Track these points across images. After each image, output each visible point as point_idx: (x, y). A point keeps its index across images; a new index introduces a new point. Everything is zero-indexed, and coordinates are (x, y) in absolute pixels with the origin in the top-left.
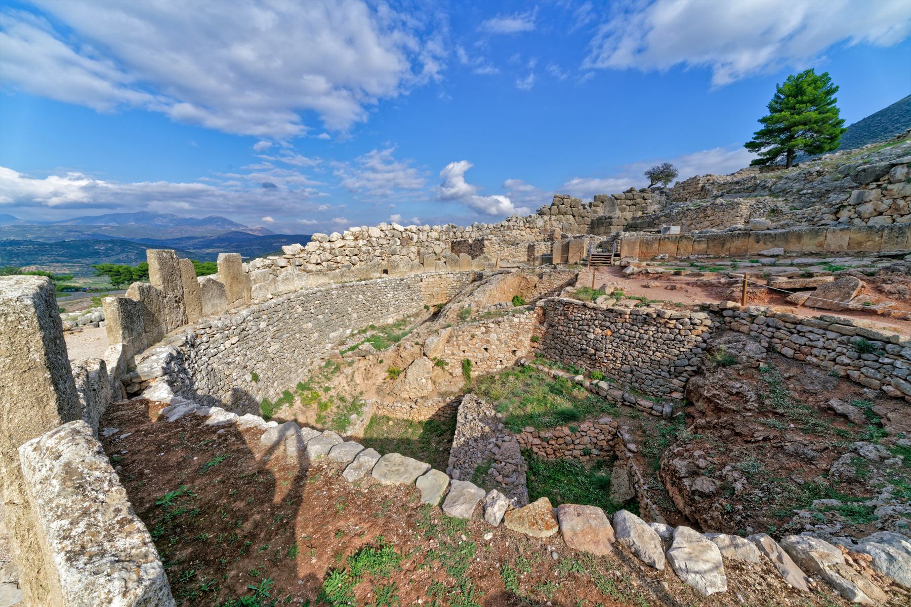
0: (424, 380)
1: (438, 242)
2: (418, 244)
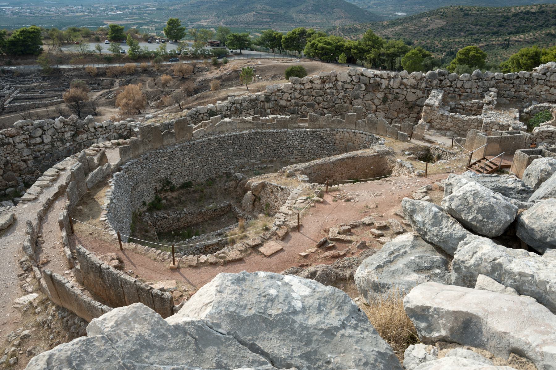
1: (413, 90)
2: (386, 91)
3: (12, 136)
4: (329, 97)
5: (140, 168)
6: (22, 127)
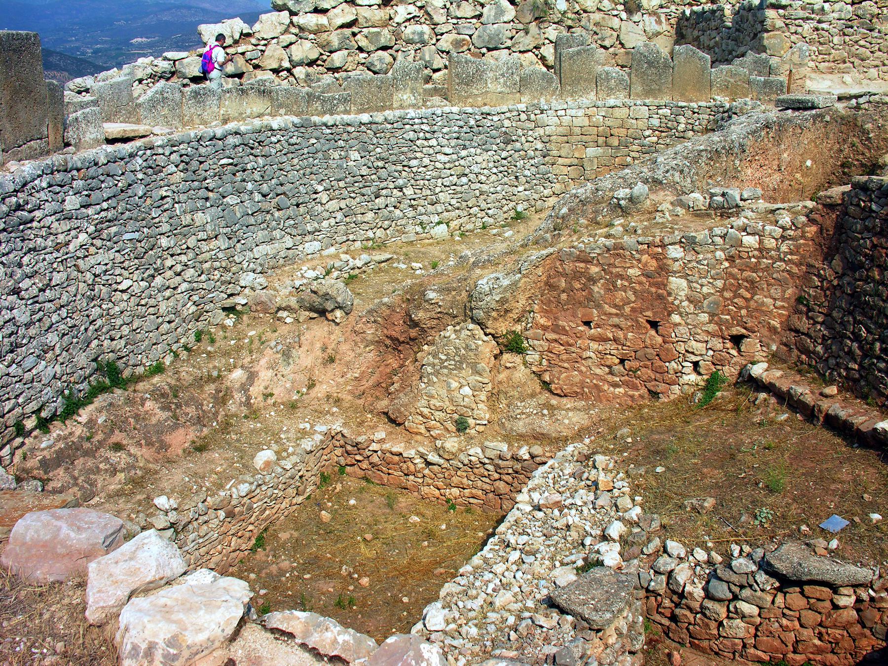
0: (467, 390)
4: (411, 47)
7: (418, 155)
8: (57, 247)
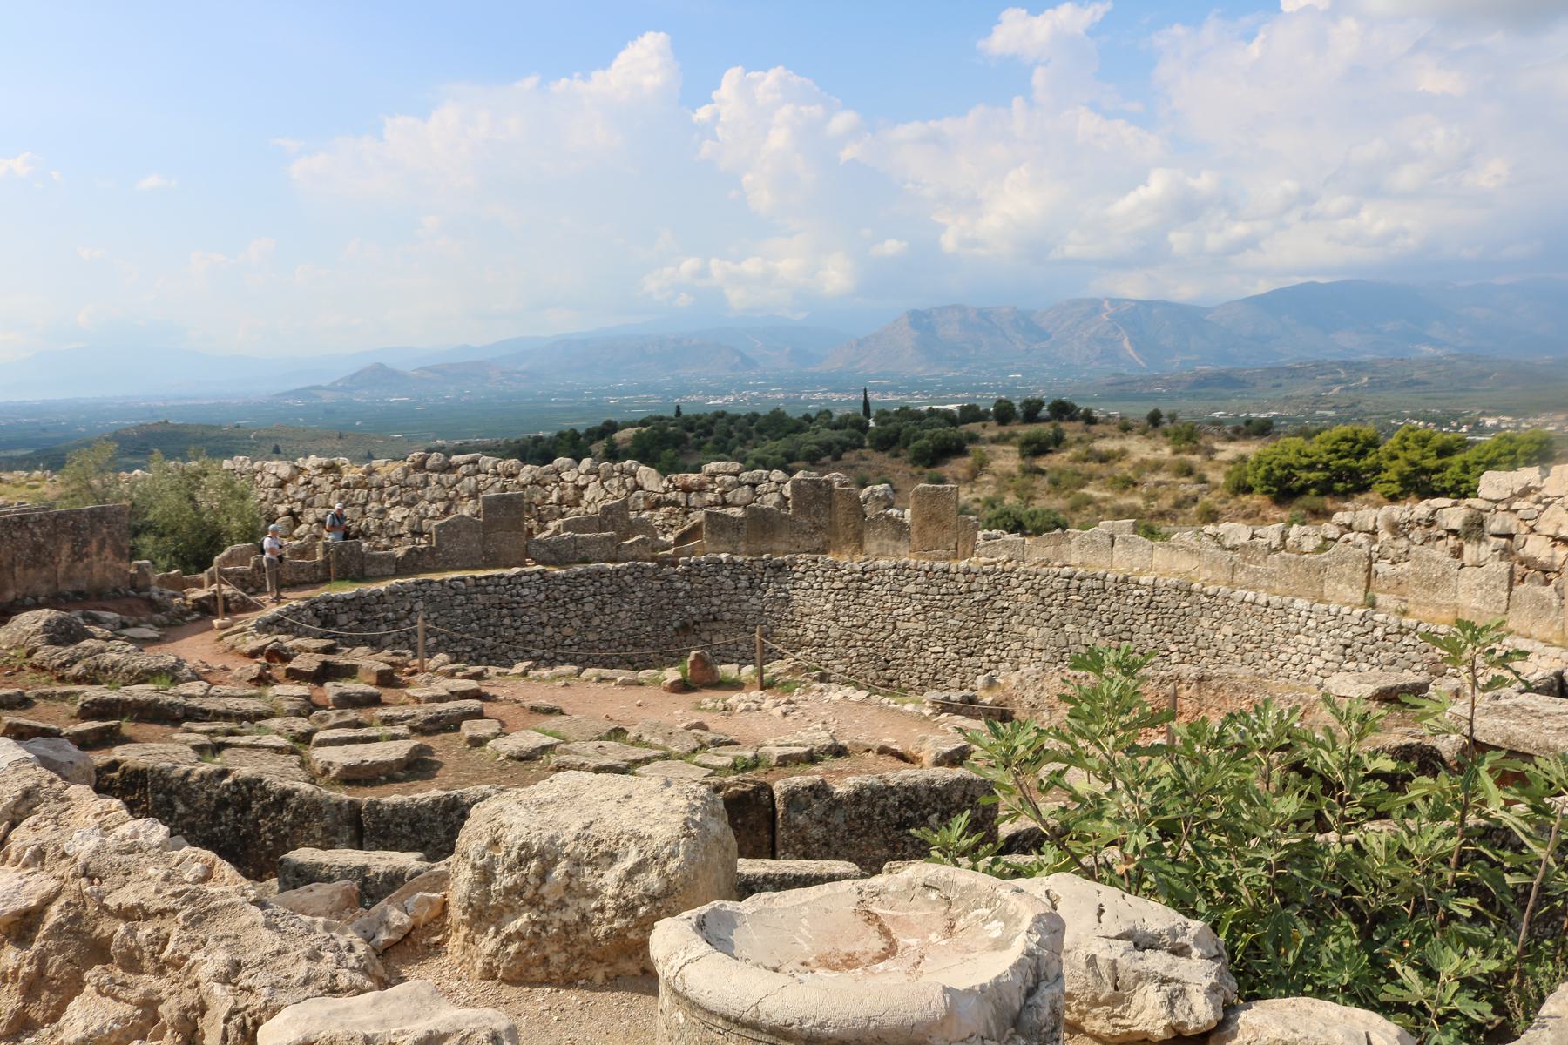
3: (687, 490)
5: (744, 583)
6: (713, 475)
7: (1291, 650)
8: (883, 609)
